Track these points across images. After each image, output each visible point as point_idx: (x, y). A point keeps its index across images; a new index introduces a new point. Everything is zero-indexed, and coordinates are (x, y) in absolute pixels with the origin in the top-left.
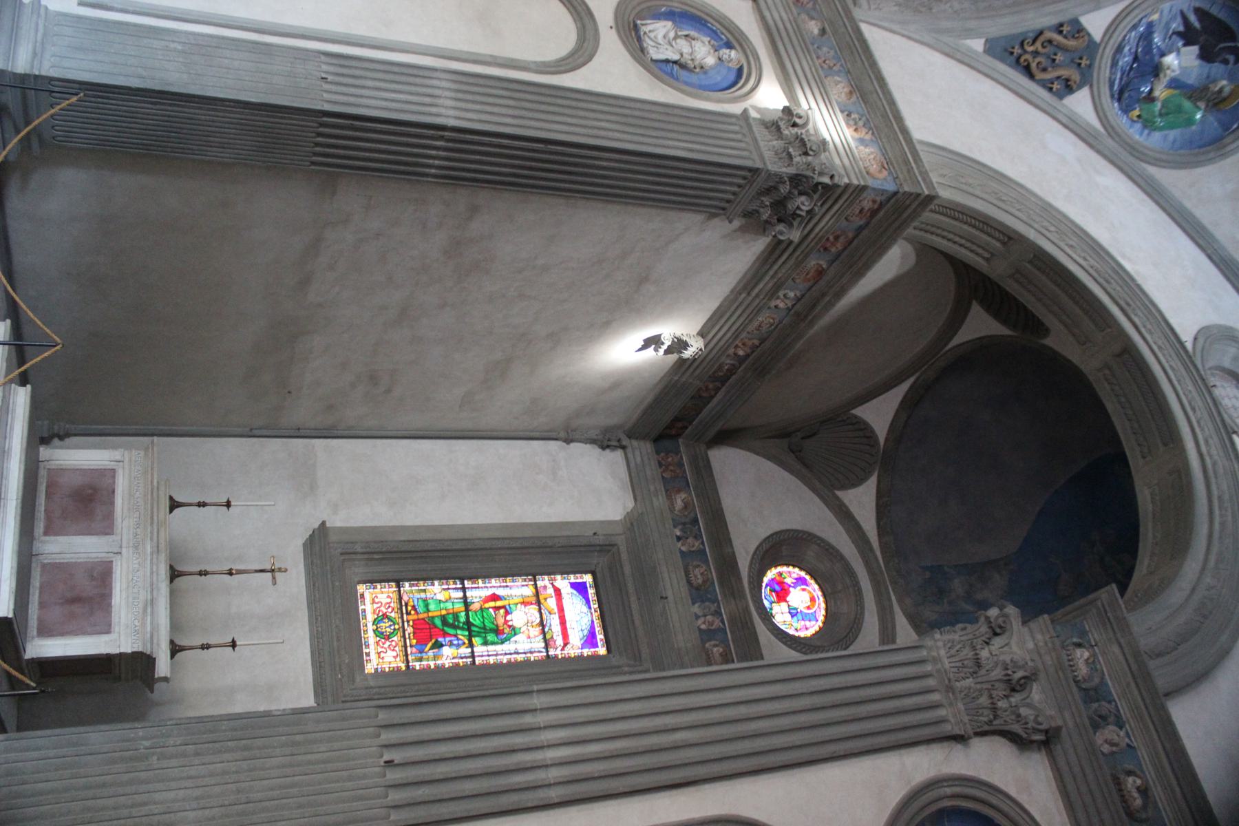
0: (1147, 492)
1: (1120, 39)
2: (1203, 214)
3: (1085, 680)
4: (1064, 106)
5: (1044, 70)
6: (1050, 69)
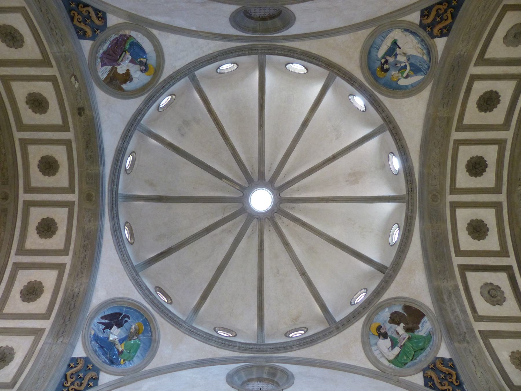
1: (91, 348)
4: (101, 385)
5: (81, 384)
6: (83, 382)
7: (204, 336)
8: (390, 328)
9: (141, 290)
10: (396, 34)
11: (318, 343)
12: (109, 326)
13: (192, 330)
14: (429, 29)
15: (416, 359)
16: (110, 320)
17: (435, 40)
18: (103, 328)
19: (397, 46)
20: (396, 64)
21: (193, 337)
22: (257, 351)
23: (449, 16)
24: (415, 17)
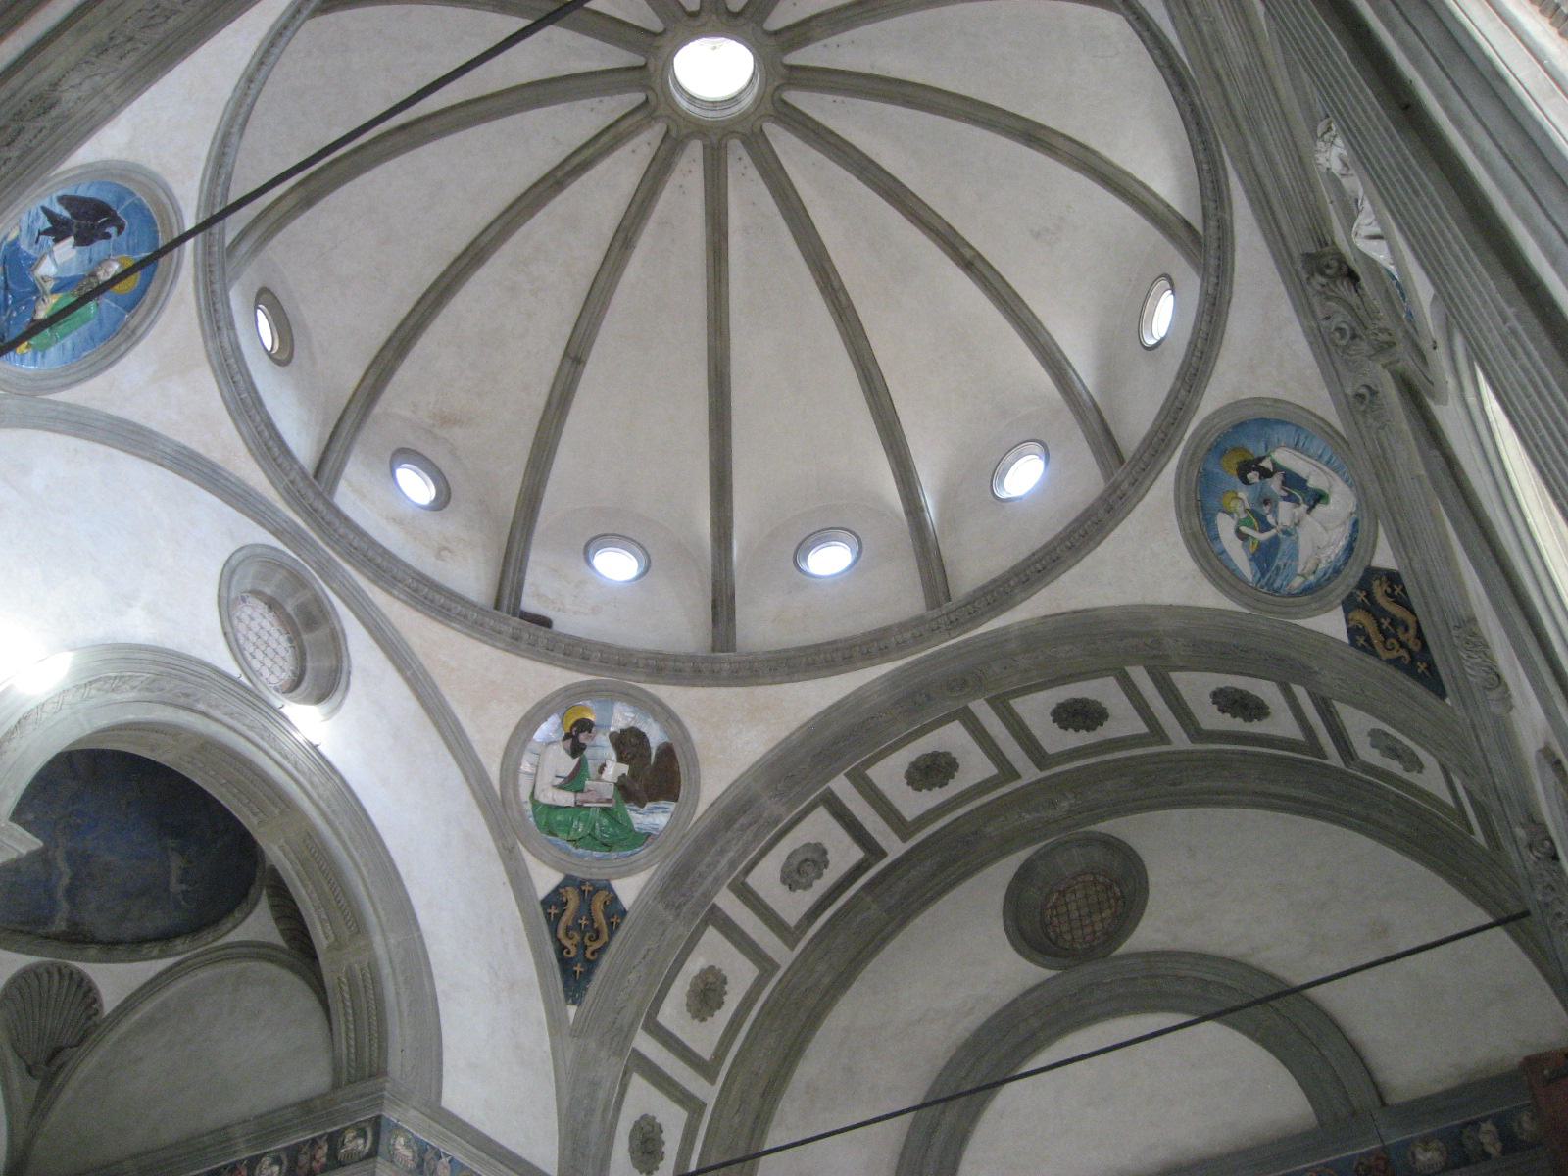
0: (276, 848)
2: (133, 412)
3: (414, 1157)
7: (243, 396)
8: (602, 748)
9: (211, 180)
10: (1341, 502)
11: (448, 626)
12: (58, 230)
13: (232, 361)
14: (1361, 596)
15: (577, 847)
16: (75, 215)
17: (1339, 612)
18: (42, 230)
19: (1312, 502)
20: (1266, 502)
21: (218, 383)
22: (319, 525)
23: (1394, 654)
24: (1384, 558)
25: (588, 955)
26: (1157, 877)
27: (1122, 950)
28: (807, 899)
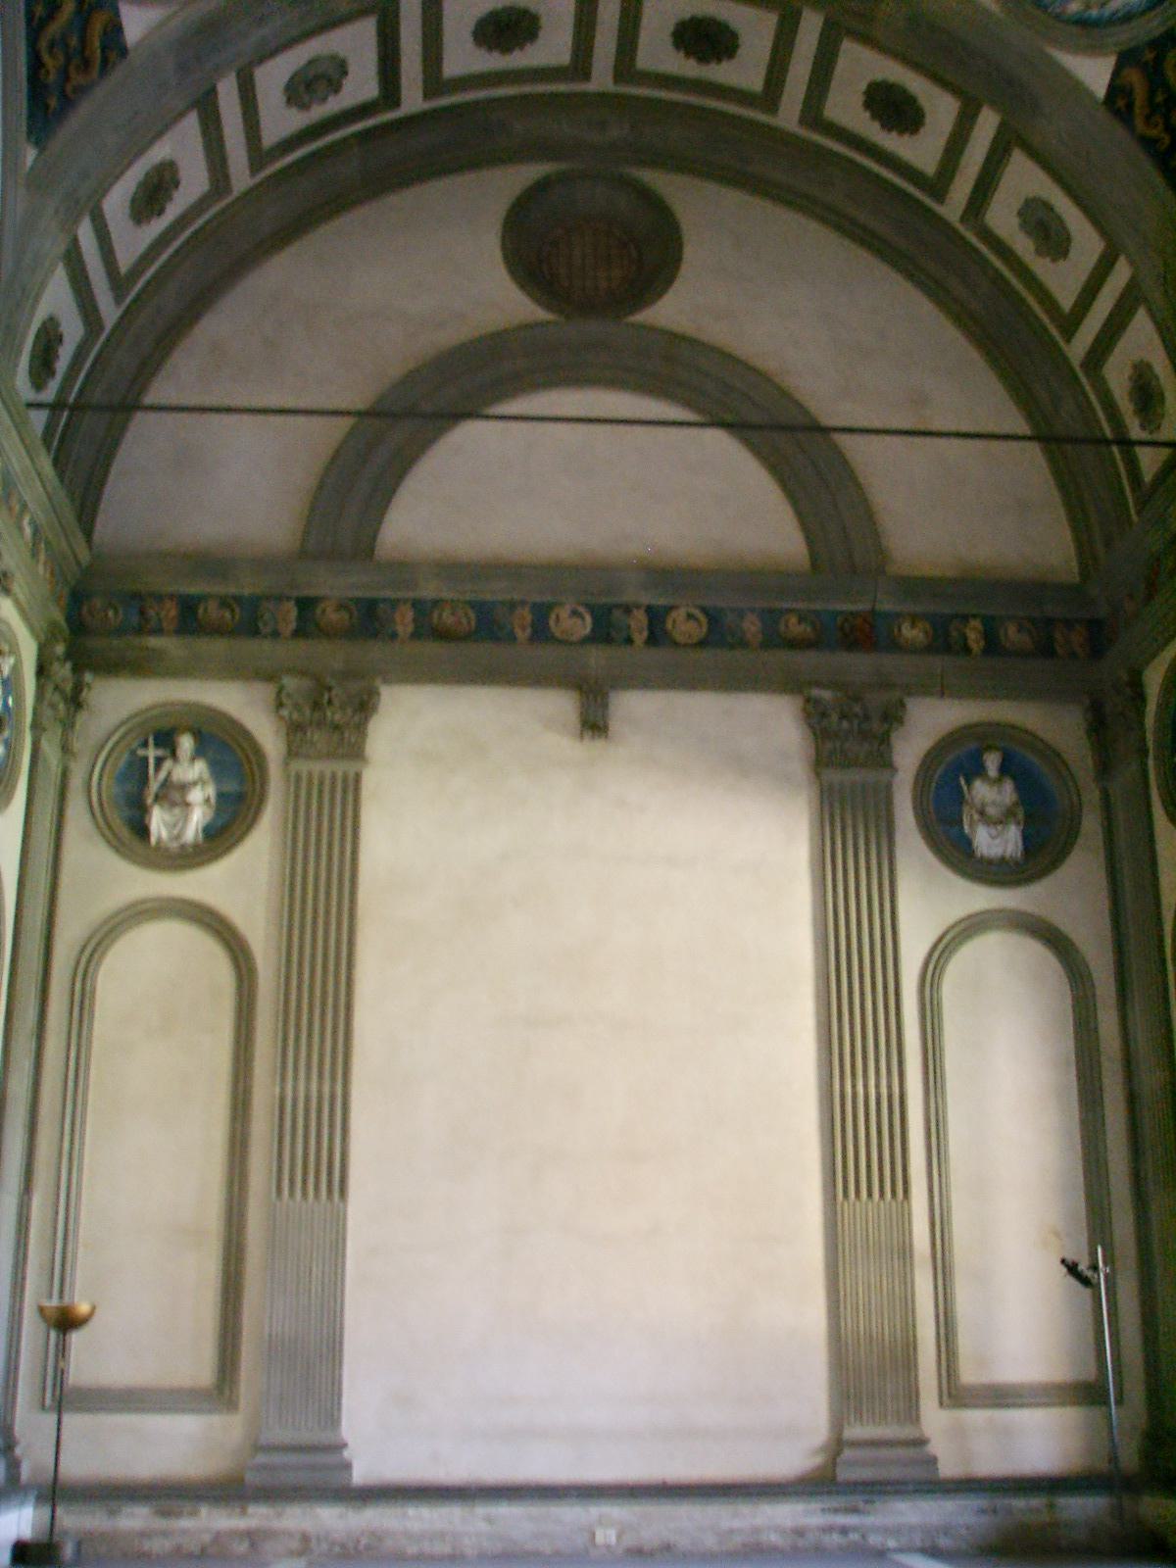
14: (1149, 56)
23: (1153, 133)
25: (69, 89)
26: (694, 253)
27: (640, 317)
28: (296, 120)
